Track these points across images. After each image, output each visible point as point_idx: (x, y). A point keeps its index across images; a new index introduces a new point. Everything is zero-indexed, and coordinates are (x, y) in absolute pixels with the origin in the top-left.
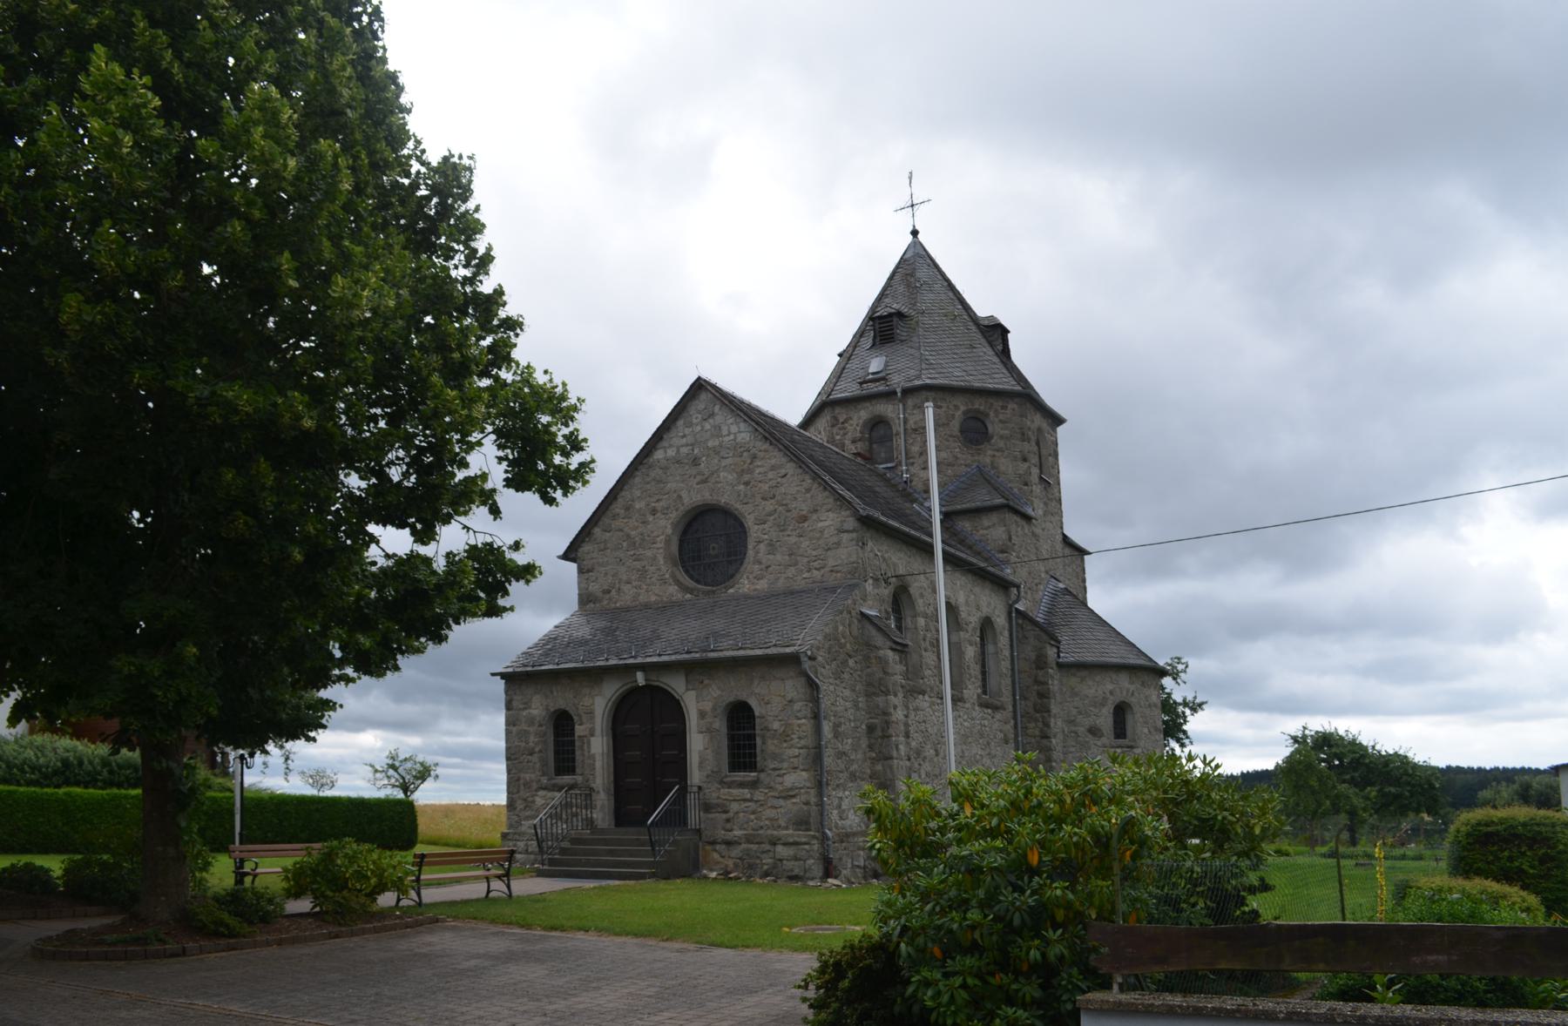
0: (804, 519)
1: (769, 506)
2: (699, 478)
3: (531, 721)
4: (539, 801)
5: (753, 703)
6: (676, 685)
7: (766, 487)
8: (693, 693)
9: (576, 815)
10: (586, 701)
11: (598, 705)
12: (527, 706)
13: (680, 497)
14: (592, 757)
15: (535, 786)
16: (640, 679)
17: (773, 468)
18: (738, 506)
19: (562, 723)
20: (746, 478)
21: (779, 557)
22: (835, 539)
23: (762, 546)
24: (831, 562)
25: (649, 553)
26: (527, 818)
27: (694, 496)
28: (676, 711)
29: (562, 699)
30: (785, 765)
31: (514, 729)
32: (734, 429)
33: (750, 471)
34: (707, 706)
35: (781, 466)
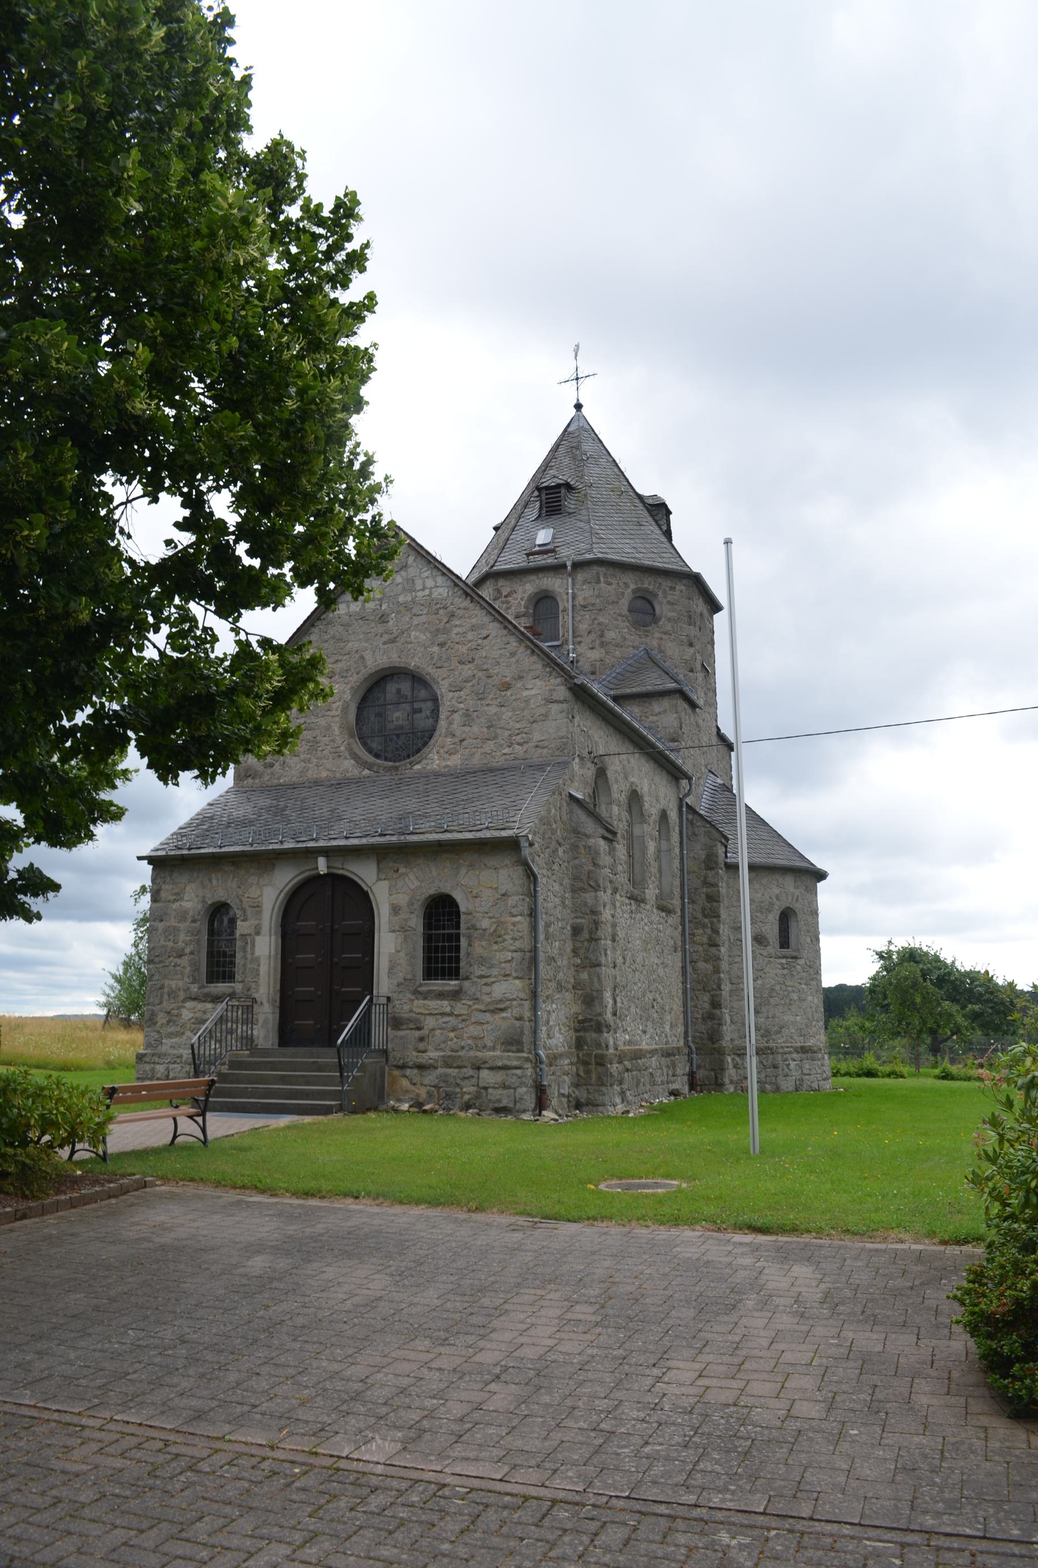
0: (507, 686)
1: (467, 670)
2: (386, 637)
3: (182, 916)
4: (186, 1015)
5: (458, 896)
6: (365, 873)
7: (464, 649)
8: (385, 884)
9: (231, 1032)
10: (253, 892)
11: (268, 894)
12: (179, 897)
13: (362, 657)
14: (257, 960)
15: (182, 995)
16: (322, 866)
17: (473, 628)
18: (430, 670)
19: (219, 915)
20: (441, 638)
21: (475, 729)
22: (543, 711)
23: (456, 716)
24: (537, 736)
25: (322, 722)
26: (170, 1035)
27: (378, 659)
28: (361, 902)
29: (221, 887)
30: (495, 971)
31: (161, 926)
32: (430, 583)
33: (446, 631)
34: (402, 899)
35: (483, 626)
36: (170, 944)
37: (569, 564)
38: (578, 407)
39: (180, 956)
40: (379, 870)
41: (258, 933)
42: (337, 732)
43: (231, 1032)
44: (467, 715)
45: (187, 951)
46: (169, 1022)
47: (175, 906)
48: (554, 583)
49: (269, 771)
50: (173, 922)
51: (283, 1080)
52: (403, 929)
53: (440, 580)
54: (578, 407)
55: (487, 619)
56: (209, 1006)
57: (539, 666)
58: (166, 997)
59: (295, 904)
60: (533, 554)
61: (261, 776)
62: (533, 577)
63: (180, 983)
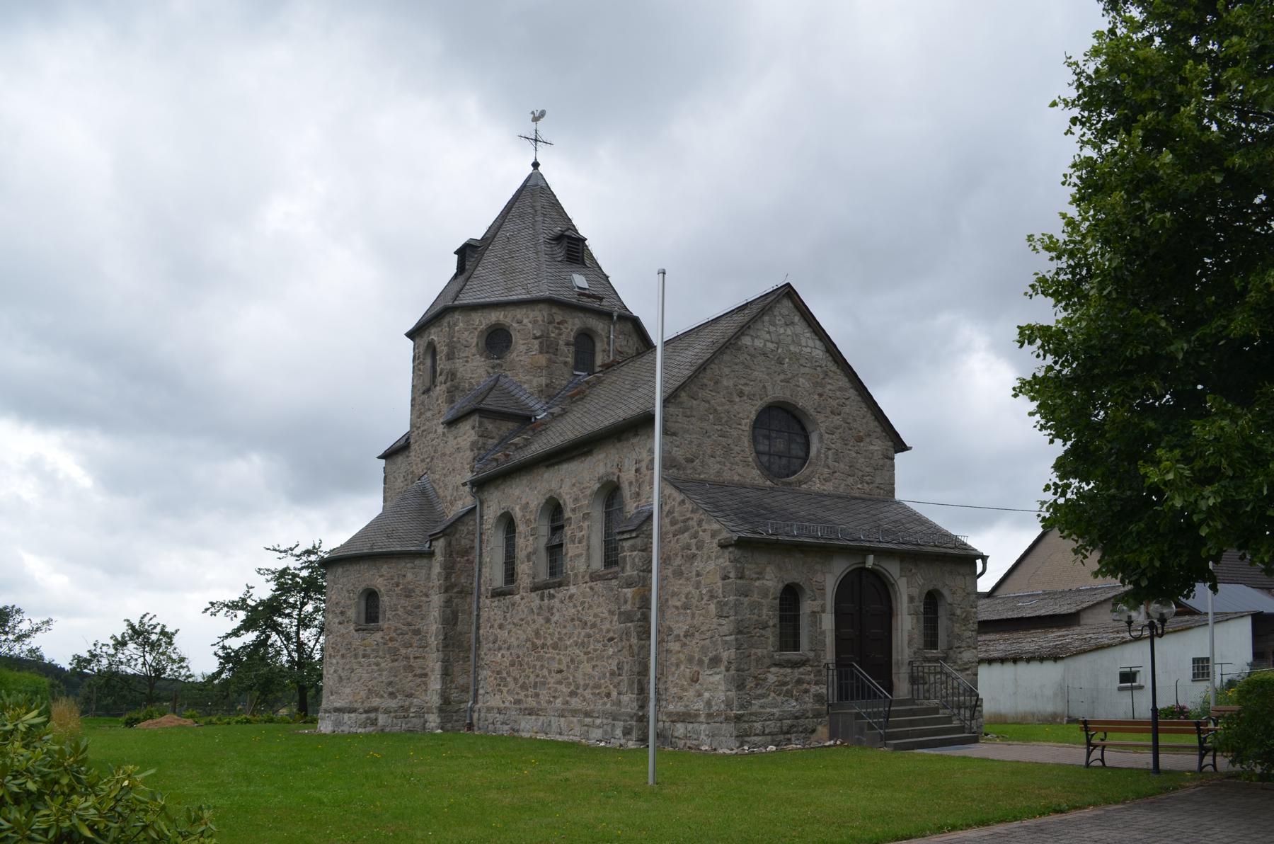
0: (860, 439)
1: (837, 420)
2: (782, 377)
3: (765, 593)
4: (772, 678)
5: (945, 592)
6: (892, 569)
7: (834, 403)
8: (904, 580)
9: (806, 691)
10: (819, 577)
11: (830, 577)
12: (760, 575)
13: (764, 387)
14: (823, 633)
15: (767, 661)
16: (870, 561)
17: (840, 389)
18: (812, 411)
19: (790, 597)
20: (820, 390)
21: (842, 466)
22: (881, 462)
23: (830, 453)
24: (878, 480)
25: (735, 433)
26: (758, 697)
27: (776, 392)
28: (883, 589)
29: (794, 571)
30: (964, 644)
31: (746, 600)
32: (811, 343)
33: (823, 386)
34: (915, 592)
35: (846, 390)
36: (756, 617)
37: (615, 315)
38: (536, 165)
39: (764, 628)
40: (901, 570)
41: (823, 611)
42: (746, 444)
43: (806, 691)
44: (836, 453)
45: (771, 623)
46: (757, 685)
47: (757, 584)
48: (598, 325)
49: (690, 465)
50: (756, 597)
51: (911, 723)
52: (916, 613)
53: (818, 343)
54: (536, 165)
55: (848, 385)
56: (789, 670)
57: (879, 430)
58: (753, 664)
59: (844, 589)
60: (584, 295)
61: (684, 469)
62: (581, 315)
63: (765, 652)
